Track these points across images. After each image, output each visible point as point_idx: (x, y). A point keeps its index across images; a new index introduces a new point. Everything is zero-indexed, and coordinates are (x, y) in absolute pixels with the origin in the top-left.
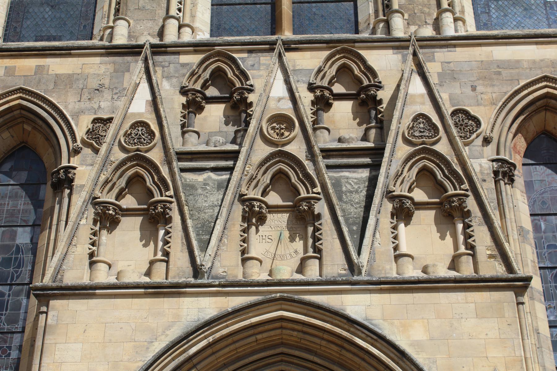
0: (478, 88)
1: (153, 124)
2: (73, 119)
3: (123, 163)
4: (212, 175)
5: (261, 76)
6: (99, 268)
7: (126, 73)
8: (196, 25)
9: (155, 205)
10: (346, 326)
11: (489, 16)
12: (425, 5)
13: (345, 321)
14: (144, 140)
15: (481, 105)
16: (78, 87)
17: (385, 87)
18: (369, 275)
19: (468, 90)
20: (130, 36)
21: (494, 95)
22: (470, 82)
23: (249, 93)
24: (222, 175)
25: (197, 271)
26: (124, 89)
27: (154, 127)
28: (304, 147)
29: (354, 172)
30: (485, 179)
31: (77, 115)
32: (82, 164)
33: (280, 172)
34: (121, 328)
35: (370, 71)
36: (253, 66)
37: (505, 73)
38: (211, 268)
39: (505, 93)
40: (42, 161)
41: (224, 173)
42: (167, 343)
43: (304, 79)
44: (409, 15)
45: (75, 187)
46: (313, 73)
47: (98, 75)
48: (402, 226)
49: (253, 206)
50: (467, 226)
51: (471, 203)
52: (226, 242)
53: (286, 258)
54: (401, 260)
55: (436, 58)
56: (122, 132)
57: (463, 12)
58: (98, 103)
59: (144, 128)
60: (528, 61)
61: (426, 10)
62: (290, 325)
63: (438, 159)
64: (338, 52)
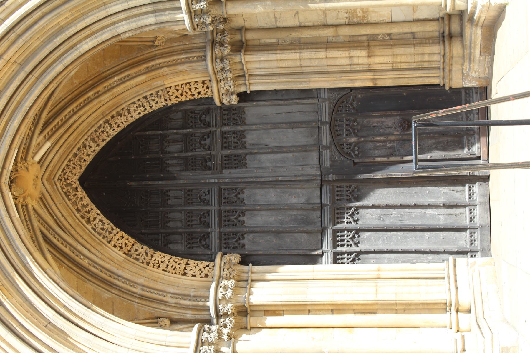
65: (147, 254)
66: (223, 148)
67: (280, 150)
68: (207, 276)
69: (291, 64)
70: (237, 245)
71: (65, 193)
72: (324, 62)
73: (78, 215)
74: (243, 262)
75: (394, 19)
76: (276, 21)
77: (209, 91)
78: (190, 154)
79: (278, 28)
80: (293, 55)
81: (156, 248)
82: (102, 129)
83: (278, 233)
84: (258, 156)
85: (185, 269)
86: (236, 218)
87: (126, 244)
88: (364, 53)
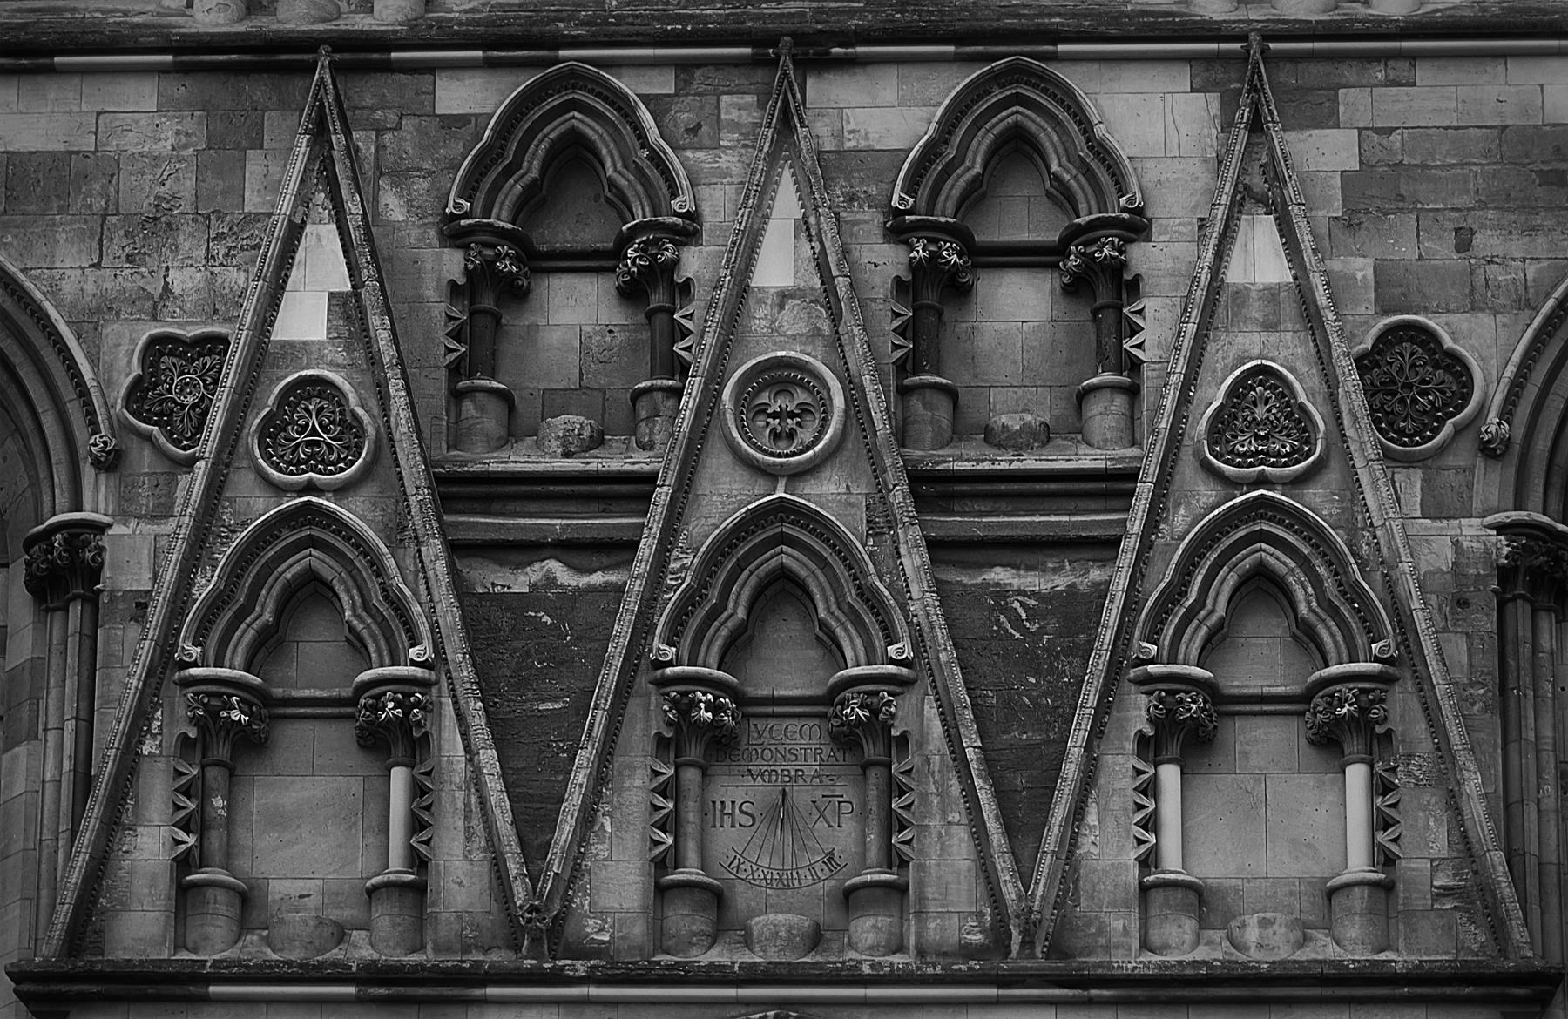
0: (1478, 239)
2: (79, 337)
5: (724, 174)
9: (377, 691)
15: (1482, 310)
16: (90, 207)
19: (1442, 250)
22: (1454, 215)
23: (679, 244)
24: (591, 572)
30: (1467, 596)
33: (783, 575)
36: (694, 130)
41: (595, 560)
43: (873, 190)
46: (906, 165)
47: (156, 160)
49: (694, 704)
50: (1380, 786)
52: (608, 829)
53: (796, 882)
55: (1341, 109)
58: (162, 273)
59: (325, 403)
63: (1307, 539)
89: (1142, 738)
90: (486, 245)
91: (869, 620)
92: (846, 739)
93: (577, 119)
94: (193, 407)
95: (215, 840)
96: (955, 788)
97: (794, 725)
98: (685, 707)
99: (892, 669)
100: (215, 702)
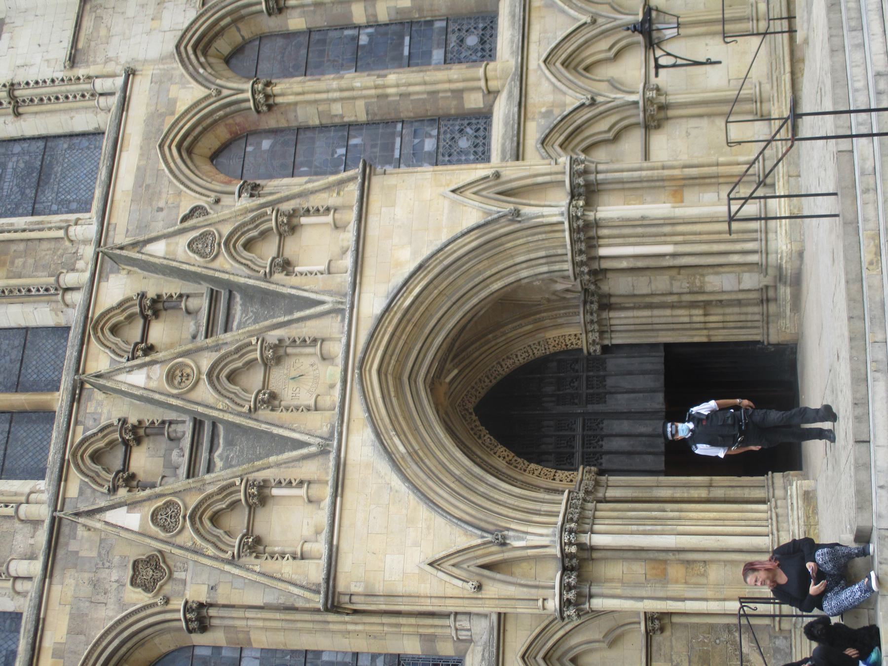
1: (155, 503)
3: (197, 531)
4: (216, 454)
5: (109, 412)
6: (309, 549)
7: (80, 555)
8: (27, 490)
9: (248, 495)
10: (392, 314)
11: (73, 201)
12: (54, 253)
13: (387, 314)
14: (173, 511)
17: (144, 290)
18: (345, 295)
19: (161, 215)
20: (32, 557)
21: (171, 192)
24: (219, 443)
25: (323, 452)
26: (99, 554)
27: (160, 503)
28: (206, 354)
29: (234, 317)
31: (122, 605)
32: (183, 595)
34: (374, 518)
35: (122, 305)
36: (95, 420)
37: (148, 181)
38: (322, 438)
39: (170, 182)
40: (167, 654)
42: (393, 473)
44: (63, 268)
45: (209, 600)
47: (77, 585)
48: (297, 269)
49: (263, 400)
50: (307, 212)
51: (287, 207)
54: (332, 270)
56: (162, 535)
57: (67, 221)
58: (111, 583)
60: (140, 160)
61: (60, 251)
62: (385, 365)
64: (95, 333)
65: (524, 464)
66: (587, 388)
67: (633, 391)
68: (571, 481)
69: (644, 321)
70: (596, 462)
71: (462, 415)
72: (670, 320)
73: (472, 432)
74: (601, 473)
75: (724, 289)
76: (634, 289)
77: (580, 342)
78: (561, 392)
79: (635, 296)
80: (647, 313)
81: (530, 461)
82: (494, 369)
83: (629, 453)
84: (615, 396)
85: (555, 475)
86: (597, 442)
87: (508, 456)
88: (701, 312)
89: (287, 275)
90: (118, 480)
91: (244, 351)
92: (278, 360)
93: (86, 456)
94: (153, 572)
95: (287, 549)
96: (295, 325)
97: (272, 376)
98: (263, 402)
99: (259, 342)
100: (246, 547)
